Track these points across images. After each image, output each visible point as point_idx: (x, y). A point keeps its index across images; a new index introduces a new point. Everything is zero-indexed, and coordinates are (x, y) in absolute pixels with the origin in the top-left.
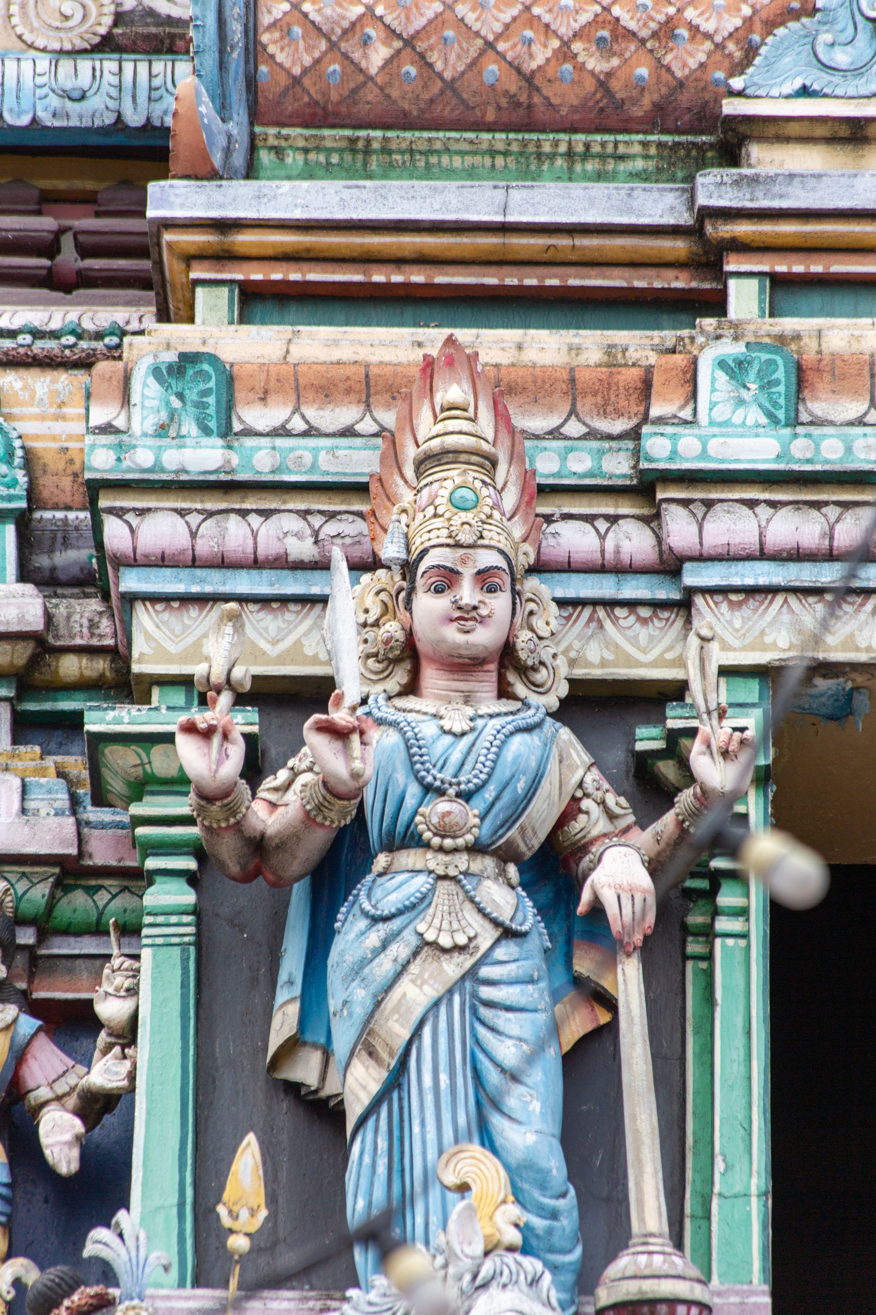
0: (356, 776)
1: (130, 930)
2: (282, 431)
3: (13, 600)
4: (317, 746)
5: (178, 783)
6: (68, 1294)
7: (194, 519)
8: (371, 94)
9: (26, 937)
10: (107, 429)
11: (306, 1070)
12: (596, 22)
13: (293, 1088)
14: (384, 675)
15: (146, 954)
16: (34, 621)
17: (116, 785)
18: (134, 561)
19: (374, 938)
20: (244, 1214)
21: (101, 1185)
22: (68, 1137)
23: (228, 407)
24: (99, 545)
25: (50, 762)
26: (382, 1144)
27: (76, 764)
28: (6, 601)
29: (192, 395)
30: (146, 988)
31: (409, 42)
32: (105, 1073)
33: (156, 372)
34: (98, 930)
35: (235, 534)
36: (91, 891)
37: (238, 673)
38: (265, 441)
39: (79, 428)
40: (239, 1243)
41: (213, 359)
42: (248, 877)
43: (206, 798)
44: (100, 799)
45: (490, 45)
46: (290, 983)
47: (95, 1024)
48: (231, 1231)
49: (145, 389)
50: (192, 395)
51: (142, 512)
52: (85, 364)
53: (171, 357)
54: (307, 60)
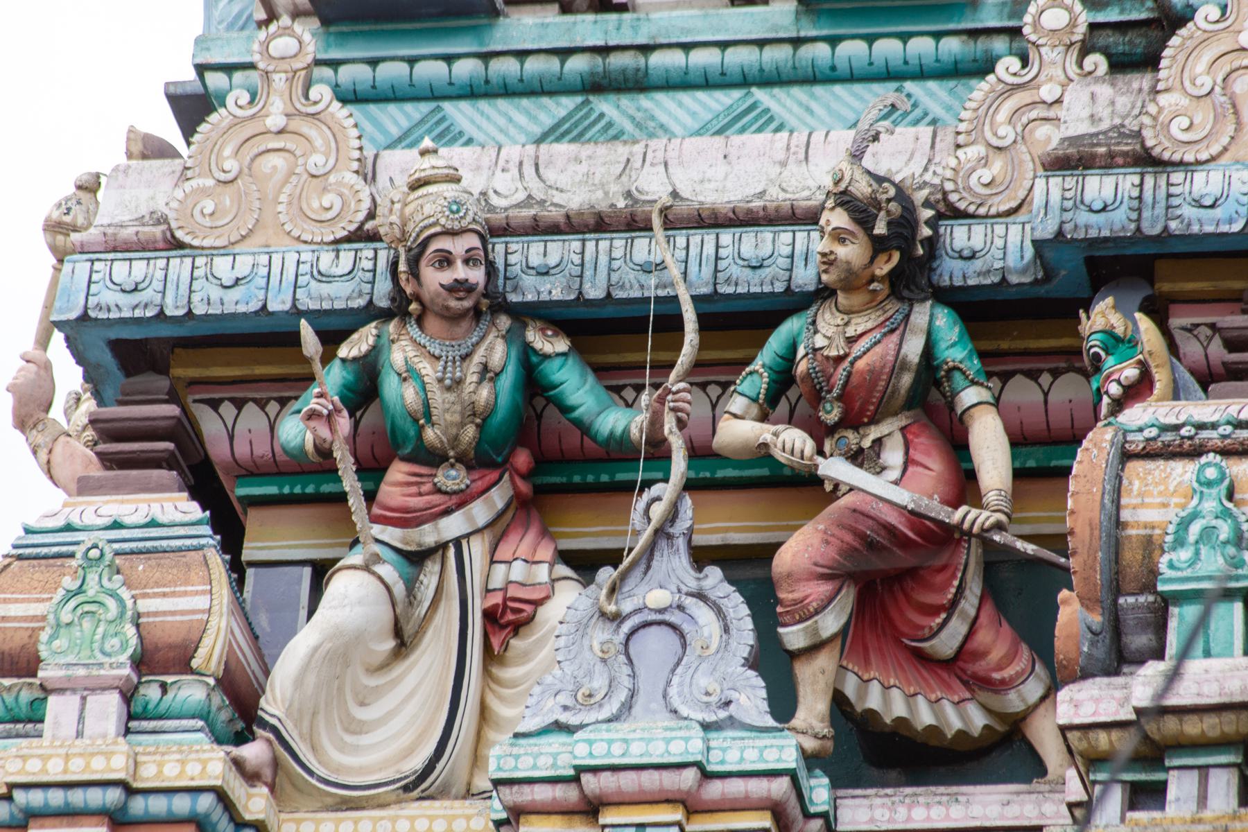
3: (1236, 673)
28: (1229, 674)
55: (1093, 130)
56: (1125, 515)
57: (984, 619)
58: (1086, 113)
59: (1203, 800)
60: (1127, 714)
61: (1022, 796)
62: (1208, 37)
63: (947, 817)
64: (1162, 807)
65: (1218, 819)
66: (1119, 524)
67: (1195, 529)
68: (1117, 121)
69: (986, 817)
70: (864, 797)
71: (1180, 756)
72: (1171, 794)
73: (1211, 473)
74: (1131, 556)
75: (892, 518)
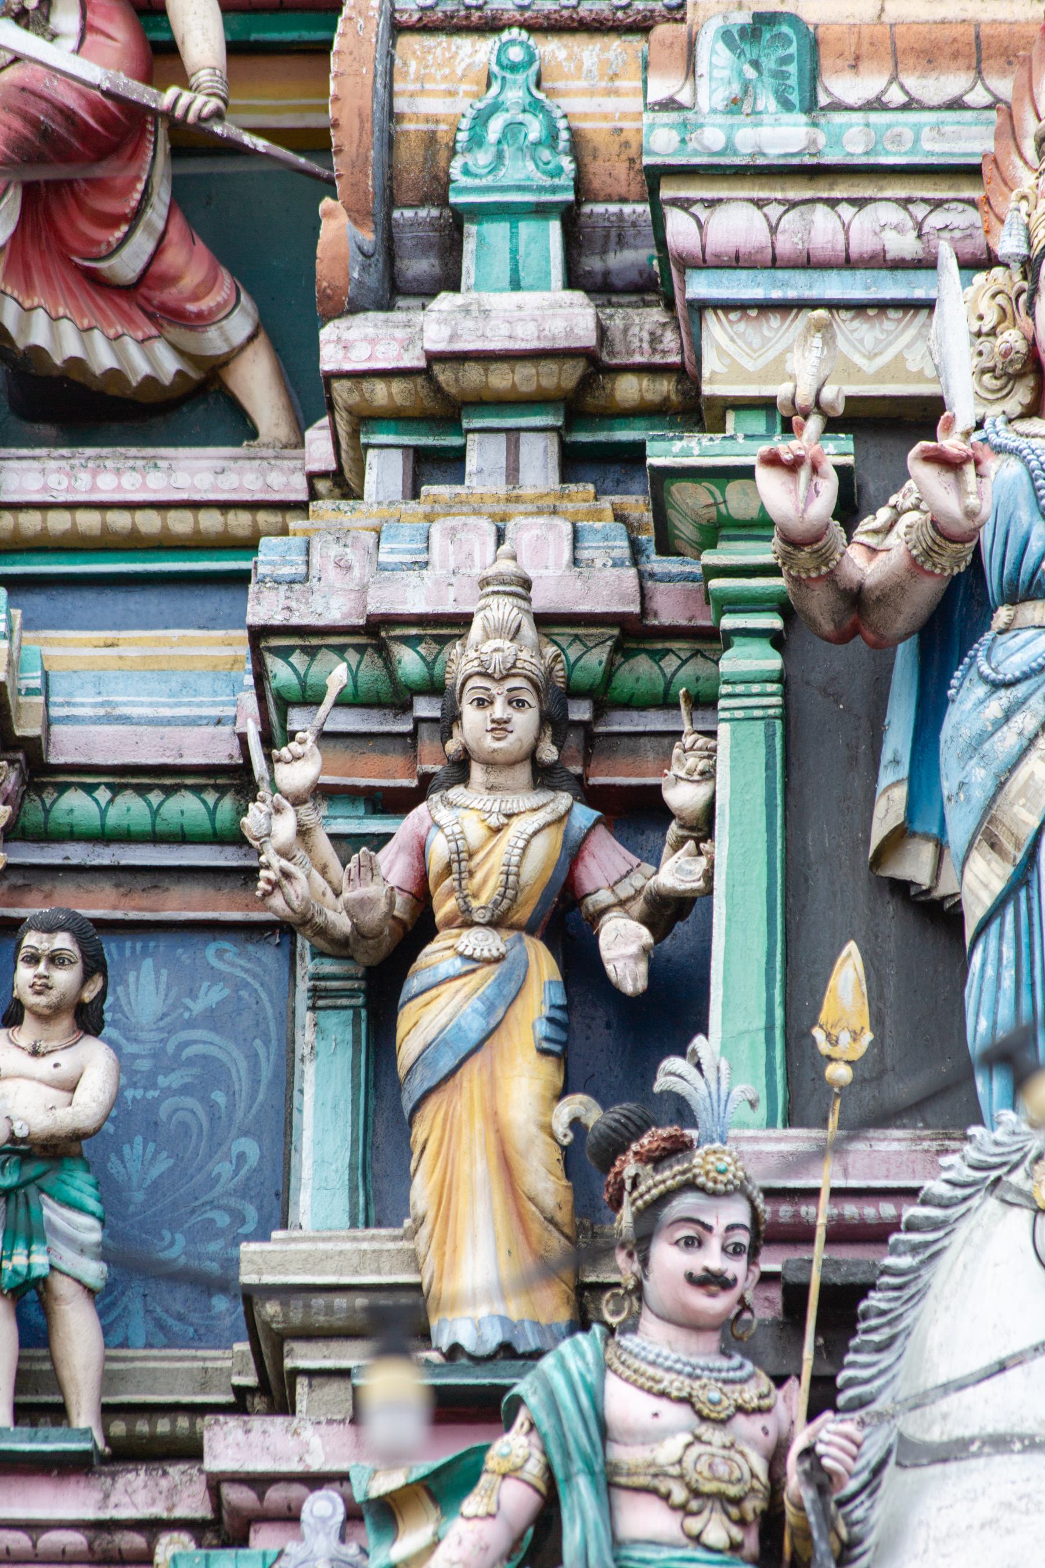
0: (971, 514)
1: (704, 702)
2: (877, 105)
3: (560, 311)
4: (924, 479)
5: (760, 525)
6: (637, 1136)
7: (774, 211)
9: (580, 711)
10: (669, 105)
11: (916, 866)
13: (901, 888)
14: (1003, 394)
15: (724, 730)
16: (585, 335)
17: (685, 530)
18: (703, 263)
19: (995, 708)
20: (845, 1038)
21: (674, 1005)
22: (634, 949)
23: (813, 77)
24: (661, 244)
25: (606, 503)
26: (1009, 953)
27: (637, 504)
28: (550, 312)
29: (769, 63)
30: (723, 769)
32: (677, 871)
33: (726, 36)
34: (666, 703)
35: (822, 228)
36: (657, 656)
37: (829, 394)
38: (857, 117)
39: (635, 104)
40: (839, 1073)
41: (794, 20)
42: (843, 637)
43: (793, 543)
44: (666, 546)
46: (896, 762)
47: (663, 814)
48: (830, 1059)
49: (713, 56)
50: (769, 63)
51: (711, 204)
52: (642, 27)
53: (744, 18)
56: (400, 105)
57: (174, 235)
59: (513, 472)
60: (414, 360)
61: (240, 463)
63: (144, 487)
64: (461, 481)
65: (541, 496)
66: (393, 116)
67: (495, 127)
69: (194, 488)
70: (34, 458)
71: (483, 417)
72: (472, 462)
73: (516, 54)
74: (409, 153)
75: (71, 100)
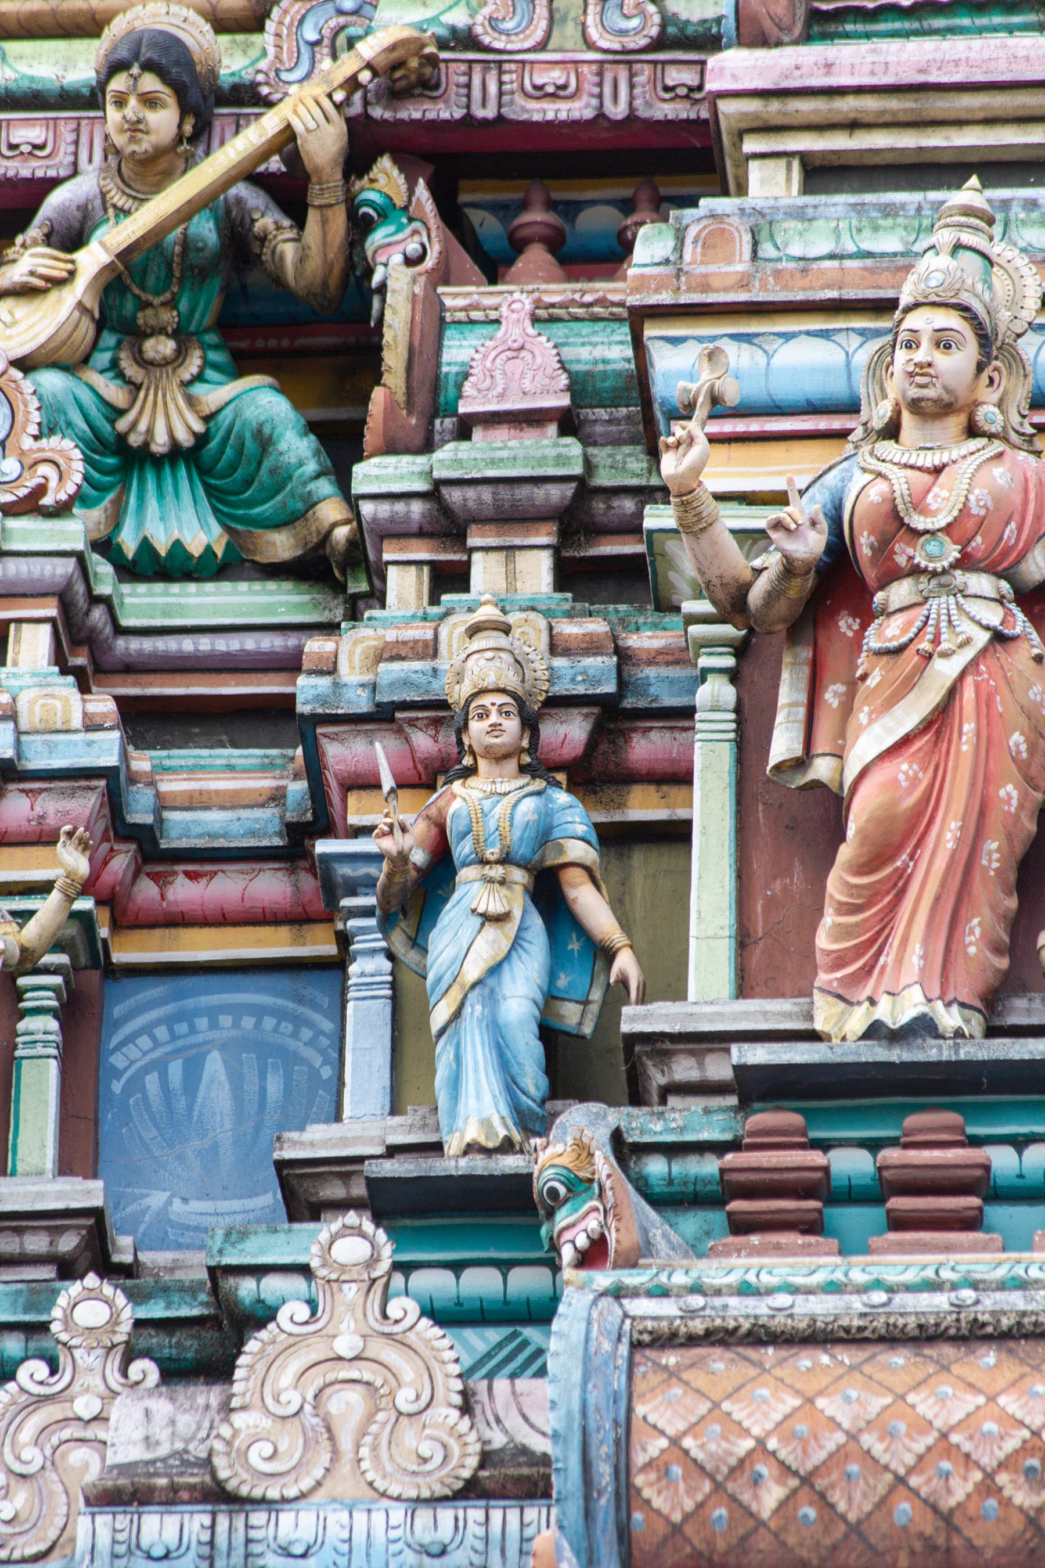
8: (763, 1542)
12: (1025, 1449)
31: (807, 1480)
45: (901, 1481)
54: (689, 1505)
55: (148, 1456)
58: (139, 1435)
62: (295, 1342)
68: (179, 1446)
